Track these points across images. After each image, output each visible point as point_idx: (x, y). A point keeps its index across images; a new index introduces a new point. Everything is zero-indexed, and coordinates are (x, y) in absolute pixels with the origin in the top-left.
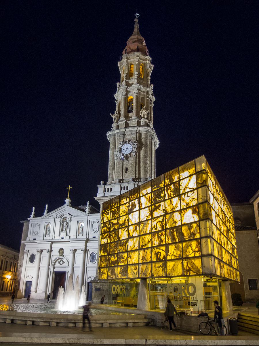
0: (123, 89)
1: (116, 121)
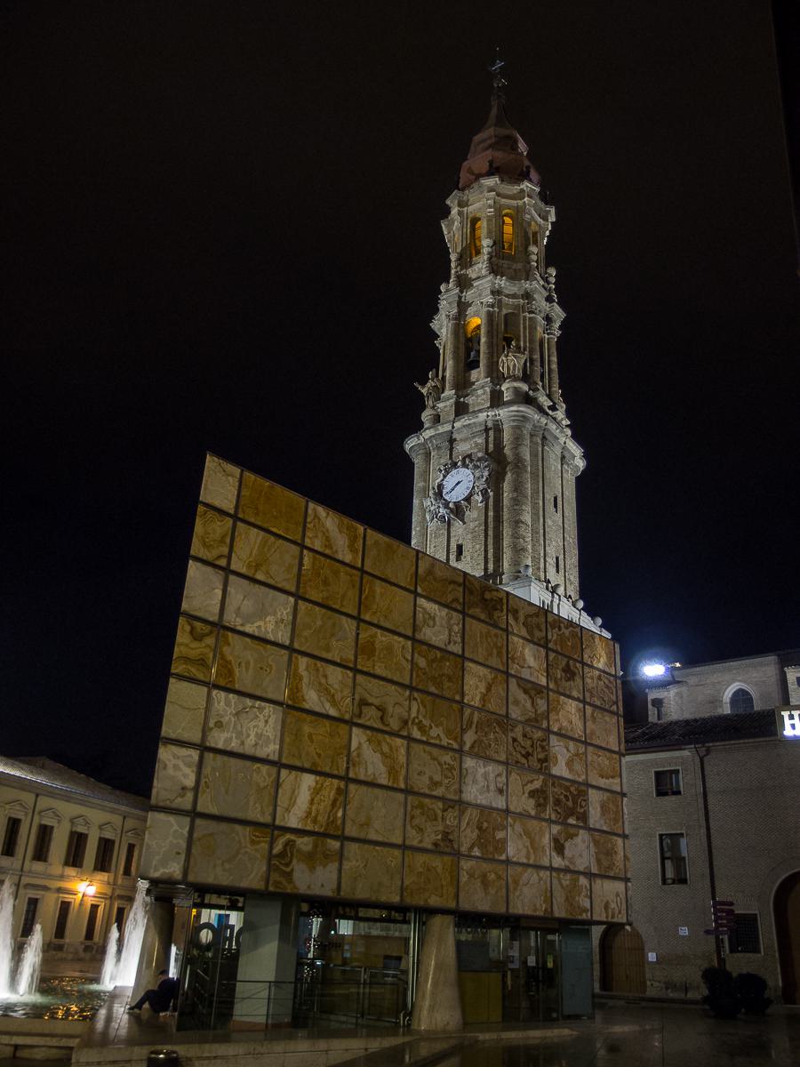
0: (450, 300)
1: (430, 402)
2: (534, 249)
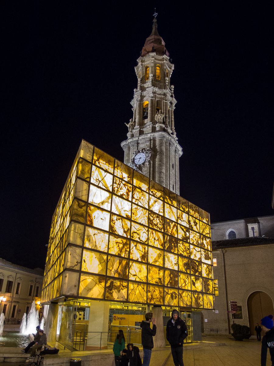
1: (130, 130)
2: (167, 79)
